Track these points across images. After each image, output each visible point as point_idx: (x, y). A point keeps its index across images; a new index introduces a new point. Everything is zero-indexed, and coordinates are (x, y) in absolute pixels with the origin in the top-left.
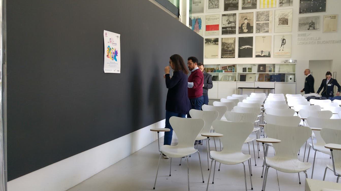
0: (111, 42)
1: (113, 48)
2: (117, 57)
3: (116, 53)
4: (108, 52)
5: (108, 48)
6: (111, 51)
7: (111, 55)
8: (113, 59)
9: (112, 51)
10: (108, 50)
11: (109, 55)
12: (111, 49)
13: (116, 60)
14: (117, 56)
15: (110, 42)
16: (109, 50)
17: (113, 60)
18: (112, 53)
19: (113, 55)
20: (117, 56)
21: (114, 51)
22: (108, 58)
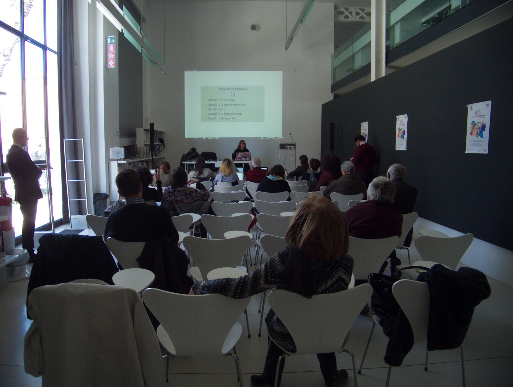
0: (477, 116)
1: (478, 122)
3: (483, 127)
4: (471, 128)
5: (472, 124)
6: (476, 127)
7: (475, 132)
8: (477, 136)
9: (478, 125)
10: (472, 126)
11: (473, 132)
12: (476, 124)
13: (482, 137)
14: (485, 130)
15: (476, 116)
17: (477, 137)
18: (476, 129)
19: (479, 131)
21: (480, 125)
22: (472, 135)
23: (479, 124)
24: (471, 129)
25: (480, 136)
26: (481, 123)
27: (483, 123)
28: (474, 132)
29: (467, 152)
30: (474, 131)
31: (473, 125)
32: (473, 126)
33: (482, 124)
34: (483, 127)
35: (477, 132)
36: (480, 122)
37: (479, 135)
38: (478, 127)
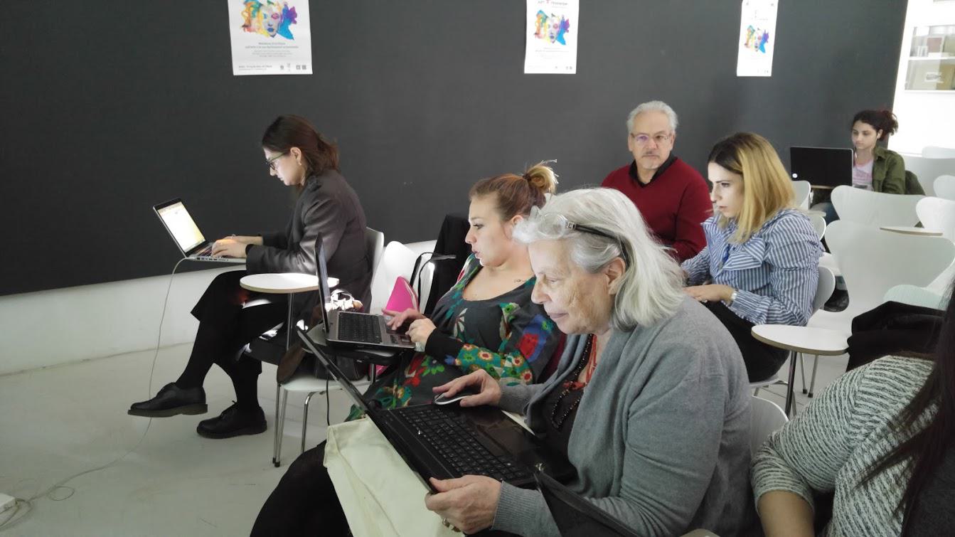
2: (292, 27)
4: (246, 15)
6: (263, 11)
8: (272, 33)
9: (270, 10)
11: (254, 23)
14: (295, 22)
16: (252, 9)
17: (273, 36)
19: (275, 23)
20: (295, 22)
23: (271, 5)
24: (244, 16)
25: (281, 34)
26: (278, 5)
27: (286, 5)
28: (257, 24)
29: (237, 71)
30: (258, 22)
31: (252, 6)
32: (252, 9)
33: (283, 7)
34: (565, 26)
35: (552, 34)
36: (275, 3)
37: (277, 32)
38: (269, 15)
